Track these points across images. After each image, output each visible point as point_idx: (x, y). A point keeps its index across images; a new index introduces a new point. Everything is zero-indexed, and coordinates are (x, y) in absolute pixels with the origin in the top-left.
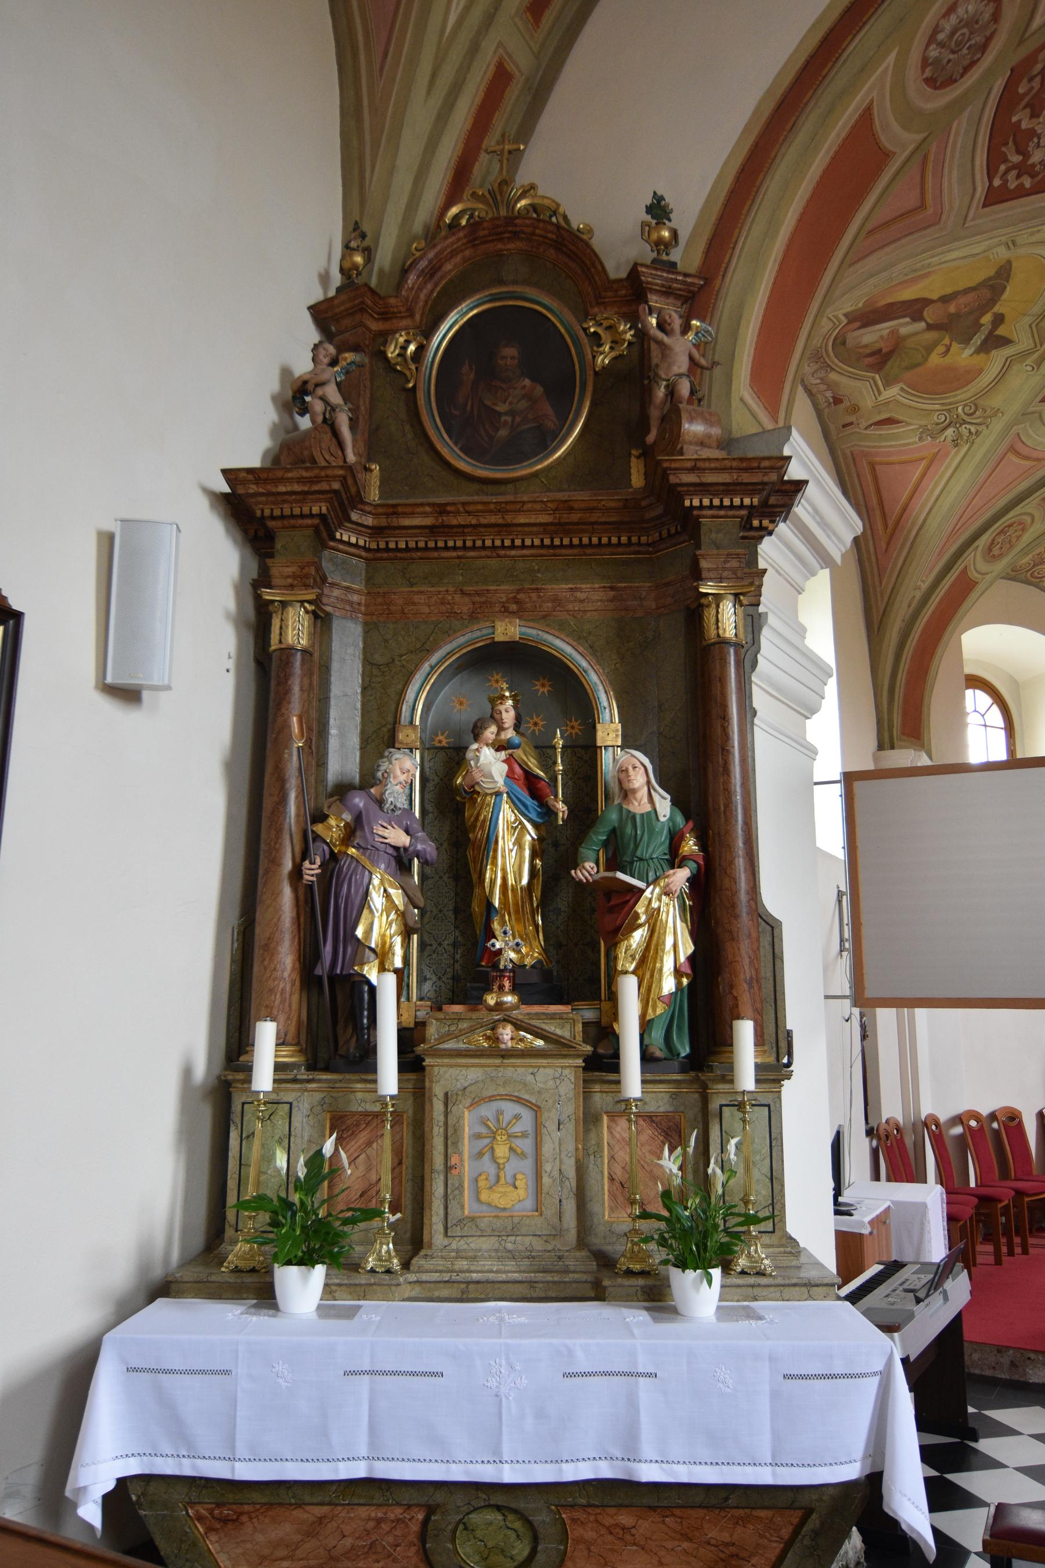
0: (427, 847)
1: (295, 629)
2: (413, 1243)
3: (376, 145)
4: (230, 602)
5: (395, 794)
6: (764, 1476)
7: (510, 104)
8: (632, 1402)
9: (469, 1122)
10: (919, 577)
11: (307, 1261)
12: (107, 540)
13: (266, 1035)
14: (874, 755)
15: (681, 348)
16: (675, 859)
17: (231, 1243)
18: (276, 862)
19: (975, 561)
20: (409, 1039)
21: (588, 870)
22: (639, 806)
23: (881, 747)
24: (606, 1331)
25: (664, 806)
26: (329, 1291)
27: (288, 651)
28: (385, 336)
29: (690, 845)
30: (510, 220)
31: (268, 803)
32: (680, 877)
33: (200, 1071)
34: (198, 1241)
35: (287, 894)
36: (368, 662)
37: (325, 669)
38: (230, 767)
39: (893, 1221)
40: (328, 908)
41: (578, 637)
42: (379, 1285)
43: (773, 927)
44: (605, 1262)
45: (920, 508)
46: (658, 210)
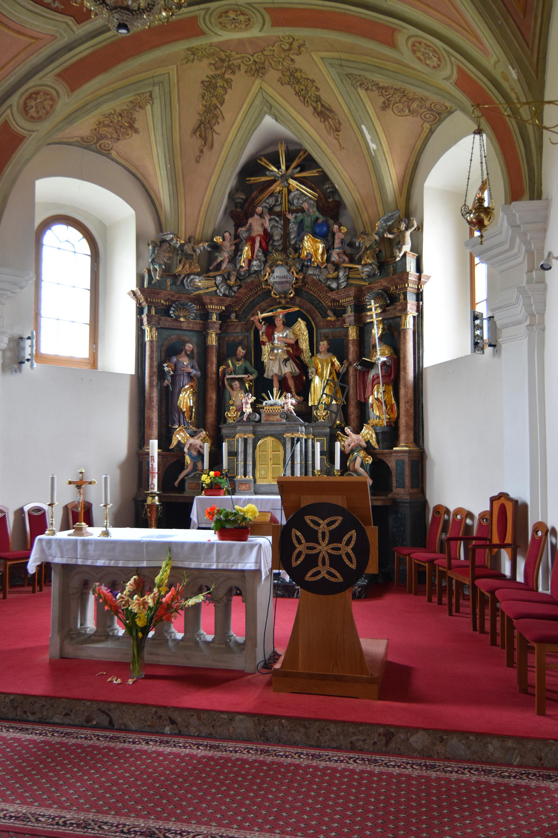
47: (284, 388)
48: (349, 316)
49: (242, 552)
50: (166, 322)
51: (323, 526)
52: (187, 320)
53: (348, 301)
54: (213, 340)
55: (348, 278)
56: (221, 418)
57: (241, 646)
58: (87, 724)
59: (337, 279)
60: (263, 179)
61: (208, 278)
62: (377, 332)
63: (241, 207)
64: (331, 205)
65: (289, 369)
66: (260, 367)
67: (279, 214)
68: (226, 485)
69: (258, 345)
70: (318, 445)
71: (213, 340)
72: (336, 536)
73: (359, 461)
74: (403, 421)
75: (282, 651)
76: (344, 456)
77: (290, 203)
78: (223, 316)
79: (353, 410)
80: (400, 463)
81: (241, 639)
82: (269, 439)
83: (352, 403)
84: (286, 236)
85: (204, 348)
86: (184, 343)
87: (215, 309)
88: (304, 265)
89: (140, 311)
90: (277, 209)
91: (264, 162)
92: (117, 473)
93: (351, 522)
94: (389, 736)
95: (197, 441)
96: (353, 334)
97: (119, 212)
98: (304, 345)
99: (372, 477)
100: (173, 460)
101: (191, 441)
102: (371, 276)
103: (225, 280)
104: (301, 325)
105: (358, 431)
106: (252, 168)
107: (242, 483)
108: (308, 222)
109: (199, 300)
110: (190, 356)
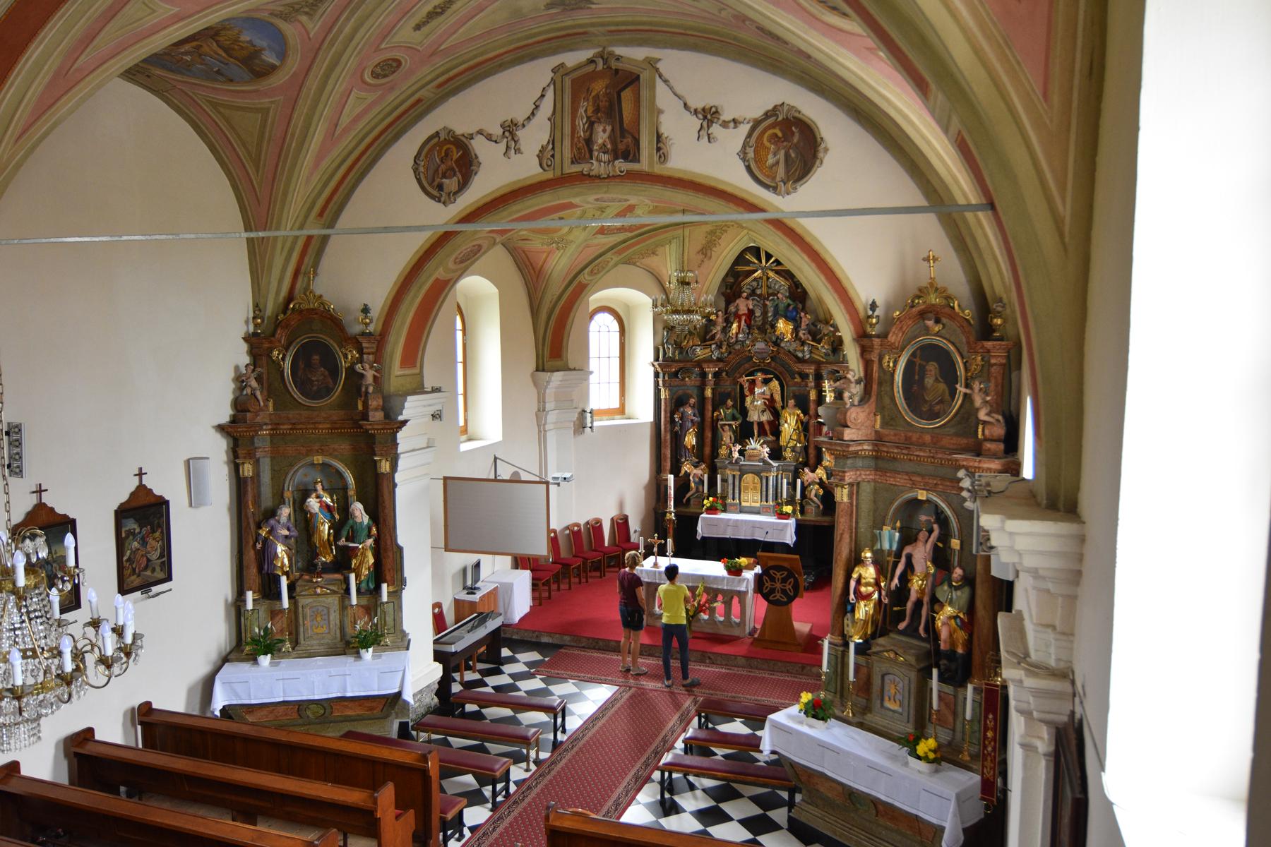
0: (295, 533)
1: (247, 470)
2: (295, 643)
4: (224, 457)
5: (284, 519)
6: (376, 693)
7: (311, 252)
8: (345, 681)
9: (308, 612)
11: (266, 654)
12: (188, 462)
13: (250, 596)
14: (533, 376)
15: (370, 375)
16: (369, 537)
17: (245, 646)
18: (247, 543)
19: (585, 277)
20: (291, 588)
21: (342, 542)
22: (359, 520)
24: (344, 664)
25: (366, 519)
26: (272, 658)
27: (246, 478)
28: (271, 350)
29: (374, 530)
30: (313, 310)
31: (244, 525)
32: (370, 541)
33: (230, 599)
34: (234, 644)
35: (252, 553)
36: (273, 470)
37: (259, 481)
38: (230, 509)
39: (500, 592)
40: (265, 556)
42: (287, 655)
43: (400, 549)
44: (348, 643)
45: (549, 267)
46: (366, 310)
47: (762, 432)
48: (811, 382)
49: (740, 581)
50: (676, 382)
51: (778, 575)
52: (691, 381)
53: (810, 370)
54: (709, 393)
55: (811, 352)
56: (715, 454)
57: (738, 625)
59: (803, 351)
60: (747, 268)
61: (706, 347)
65: (766, 417)
66: (744, 412)
67: (759, 296)
68: (719, 507)
69: (743, 397)
70: (785, 481)
71: (709, 393)
72: (784, 580)
75: (758, 626)
76: (804, 488)
78: (716, 375)
79: (812, 452)
81: (738, 620)
84: (765, 313)
85: (702, 399)
87: (711, 370)
88: (777, 342)
89: (657, 375)
90: (758, 292)
91: (749, 256)
92: (643, 493)
93: (791, 575)
94: (803, 668)
95: (698, 472)
96: (813, 395)
97: (640, 303)
98: (778, 397)
101: (695, 471)
102: (826, 354)
103: (719, 347)
104: (775, 383)
105: (813, 471)
106: (740, 260)
107: (731, 505)
108: (782, 306)
109: (699, 364)
110: (693, 407)
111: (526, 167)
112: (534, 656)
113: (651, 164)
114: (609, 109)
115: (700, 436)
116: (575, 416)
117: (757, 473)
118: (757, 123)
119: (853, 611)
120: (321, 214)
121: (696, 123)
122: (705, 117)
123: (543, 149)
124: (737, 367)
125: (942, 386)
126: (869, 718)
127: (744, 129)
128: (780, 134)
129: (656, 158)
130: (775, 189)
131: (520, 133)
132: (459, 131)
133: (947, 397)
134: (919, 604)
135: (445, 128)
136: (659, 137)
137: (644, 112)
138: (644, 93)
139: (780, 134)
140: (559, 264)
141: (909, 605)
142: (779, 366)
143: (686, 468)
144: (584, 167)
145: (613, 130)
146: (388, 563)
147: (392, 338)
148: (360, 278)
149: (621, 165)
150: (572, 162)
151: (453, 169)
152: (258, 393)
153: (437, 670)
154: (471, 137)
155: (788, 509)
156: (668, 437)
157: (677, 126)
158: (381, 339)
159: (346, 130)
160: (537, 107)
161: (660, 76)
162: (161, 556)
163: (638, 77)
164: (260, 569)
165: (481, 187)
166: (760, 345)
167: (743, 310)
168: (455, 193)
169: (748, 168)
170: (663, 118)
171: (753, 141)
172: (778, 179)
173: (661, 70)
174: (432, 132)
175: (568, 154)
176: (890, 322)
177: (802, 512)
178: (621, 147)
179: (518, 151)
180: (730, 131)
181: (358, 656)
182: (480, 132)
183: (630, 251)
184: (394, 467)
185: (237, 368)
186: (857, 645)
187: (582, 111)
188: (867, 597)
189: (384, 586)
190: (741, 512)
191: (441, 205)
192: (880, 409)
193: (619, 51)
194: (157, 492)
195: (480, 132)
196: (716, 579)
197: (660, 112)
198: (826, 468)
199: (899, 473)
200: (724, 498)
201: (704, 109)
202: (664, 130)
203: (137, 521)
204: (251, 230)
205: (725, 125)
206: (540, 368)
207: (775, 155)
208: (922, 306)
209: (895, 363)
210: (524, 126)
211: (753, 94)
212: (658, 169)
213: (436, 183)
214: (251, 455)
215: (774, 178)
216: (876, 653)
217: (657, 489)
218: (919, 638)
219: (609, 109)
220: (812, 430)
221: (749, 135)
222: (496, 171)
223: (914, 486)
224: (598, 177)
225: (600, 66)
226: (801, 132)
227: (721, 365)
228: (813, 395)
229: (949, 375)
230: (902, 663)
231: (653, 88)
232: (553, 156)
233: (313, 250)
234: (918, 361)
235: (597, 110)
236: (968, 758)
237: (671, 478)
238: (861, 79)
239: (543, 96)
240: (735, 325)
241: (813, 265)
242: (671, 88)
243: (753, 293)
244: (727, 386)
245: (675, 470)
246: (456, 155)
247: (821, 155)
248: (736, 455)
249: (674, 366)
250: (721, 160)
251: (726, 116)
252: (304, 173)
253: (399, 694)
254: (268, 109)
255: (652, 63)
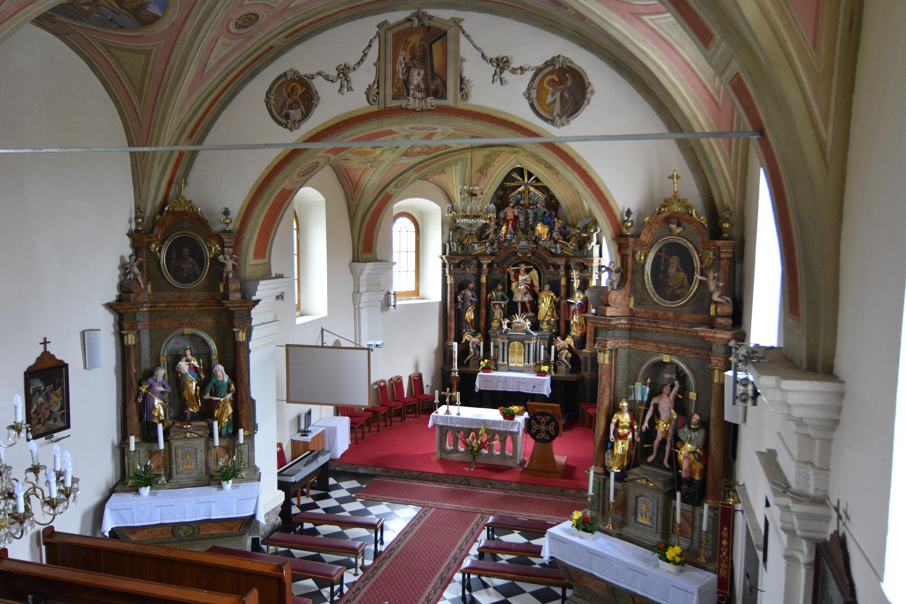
0: (169, 389)
1: (131, 339)
2: (169, 477)
3: (143, 180)
4: (112, 329)
5: (160, 379)
6: (235, 516)
9: (180, 452)
10: (367, 199)
11: (146, 486)
12: (83, 333)
13: (132, 440)
14: (350, 265)
15: (230, 264)
16: (229, 392)
17: (127, 480)
19: (391, 189)
20: (166, 433)
21: (207, 396)
22: (220, 379)
23: (353, 261)
24: (210, 492)
25: (226, 378)
26: (151, 489)
27: (129, 346)
28: (150, 244)
29: (233, 387)
30: (185, 212)
31: (128, 383)
32: (229, 396)
33: (116, 442)
34: (119, 478)
35: (134, 405)
36: (151, 339)
37: (140, 348)
38: (116, 371)
39: (326, 434)
40: (145, 408)
41: (207, 332)
42: (163, 487)
44: (211, 476)
46: (226, 212)
47: (524, 310)
49: (513, 425)
50: (458, 271)
51: (543, 420)
52: (470, 271)
53: (561, 262)
54: (484, 279)
55: (562, 249)
57: (511, 457)
58: (460, 483)
59: (556, 248)
60: (513, 184)
62: (576, 284)
63: (501, 199)
64: (552, 204)
65: (527, 298)
66: (511, 294)
67: (523, 205)
68: (493, 367)
69: (510, 283)
70: (542, 347)
71: (484, 279)
72: (548, 424)
73: (564, 355)
74: (588, 336)
75: (527, 459)
76: (556, 352)
77: (530, 199)
78: (489, 265)
79: (562, 324)
80: (586, 358)
81: (511, 454)
82: (516, 342)
83: (562, 320)
84: (527, 219)
85: (478, 284)
86: (469, 282)
87: (485, 262)
88: (536, 241)
89: (444, 265)
90: (522, 202)
91: (514, 175)
92: (433, 356)
93: (553, 419)
94: (563, 491)
95: (476, 340)
96: (563, 282)
97: (433, 212)
98: (536, 283)
99: (571, 363)
100: (464, 351)
101: (473, 339)
102: (574, 250)
103: (492, 244)
105: (564, 339)
106: (508, 177)
107: (502, 365)
108: (540, 214)
109: (477, 257)
110: (472, 290)
111: (355, 101)
112: (354, 484)
113: (455, 101)
114: (423, 58)
115: (477, 313)
116: (382, 297)
117: (521, 341)
118: (539, 70)
119: (612, 448)
120: (190, 136)
121: (491, 69)
122: (498, 65)
123: (370, 88)
124: (506, 259)
125: (682, 275)
126: (626, 530)
127: (529, 75)
128: (557, 79)
129: (459, 96)
130: (552, 122)
131: (352, 75)
132: (302, 72)
133: (686, 283)
134: (663, 442)
135: (291, 70)
136: (462, 80)
137: (451, 61)
138: (451, 46)
139: (557, 79)
140: (372, 179)
141: (656, 443)
142: (537, 259)
143: (467, 337)
144: (403, 103)
145: (425, 74)
146: (243, 413)
147: (247, 236)
148: (222, 186)
149: (432, 101)
150: (393, 99)
151: (297, 102)
152: (139, 278)
153: (281, 496)
154: (312, 77)
155: (545, 368)
156: (453, 313)
157: (477, 72)
158: (238, 236)
159: (213, 70)
160: (365, 55)
161: (463, 32)
162: (62, 409)
163: (446, 33)
164: (141, 418)
165: (320, 118)
166: (523, 243)
167: (510, 216)
168: (300, 121)
169: (532, 105)
170: (465, 65)
171: (535, 84)
172: (555, 114)
173: (464, 28)
174: (282, 72)
175: (389, 92)
176: (640, 226)
177: (555, 370)
178: (432, 87)
179: (350, 89)
180: (518, 76)
181: (220, 486)
182: (320, 74)
183: (426, 168)
184: (249, 337)
185: (122, 258)
186: (616, 474)
187: (401, 58)
188: (624, 437)
189: (241, 431)
190: (509, 371)
191: (288, 130)
192: (633, 292)
193: (431, 12)
194: (58, 357)
195: (320, 74)
196: (495, 422)
197: (463, 60)
198: (573, 337)
199: (647, 341)
200: (496, 360)
201: (497, 59)
202: (466, 74)
203: (42, 380)
204: (134, 146)
205: (514, 71)
206: (356, 260)
207: (553, 95)
208: (665, 214)
209: (646, 257)
210: (354, 69)
211: (536, 47)
212: (461, 105)
213: (284, 113)
214: (133, 327)
215: (552, 114)
216: (631, 480)
217: (444, 353)
218: (664, 468)
219: (423, 58)
220: (562, 307)
221: (533, 80)
222: (332, 105)
223: (660, 351)
224: (414, 110)
225: (416, 23)
226: (573, 78)
227: (493, 258)
228: (563, 282)
229: (687, 266)
230: (652, 488)
231: (457, 41)
232: (378, 93)
233: (184, 163)
234: (663, 255)
235: (413, 58)
236: (704, 561)
237: (455, 344)
238: (626, 37)
239: (370, 46)
240: (504, 228)
241: (582, 181)
242: (472, 42)
243: (518, 203)
244: (497, 274)
245: (458, 338)
246: (300, 91)
247: (588, 96)
248: (505, 327)
249: (457, 259)
250: (511, 99)
251: (515, 65)
252: (178, 104)
253: (253, 517)
254: (151, 51)
255: (457, 22)
